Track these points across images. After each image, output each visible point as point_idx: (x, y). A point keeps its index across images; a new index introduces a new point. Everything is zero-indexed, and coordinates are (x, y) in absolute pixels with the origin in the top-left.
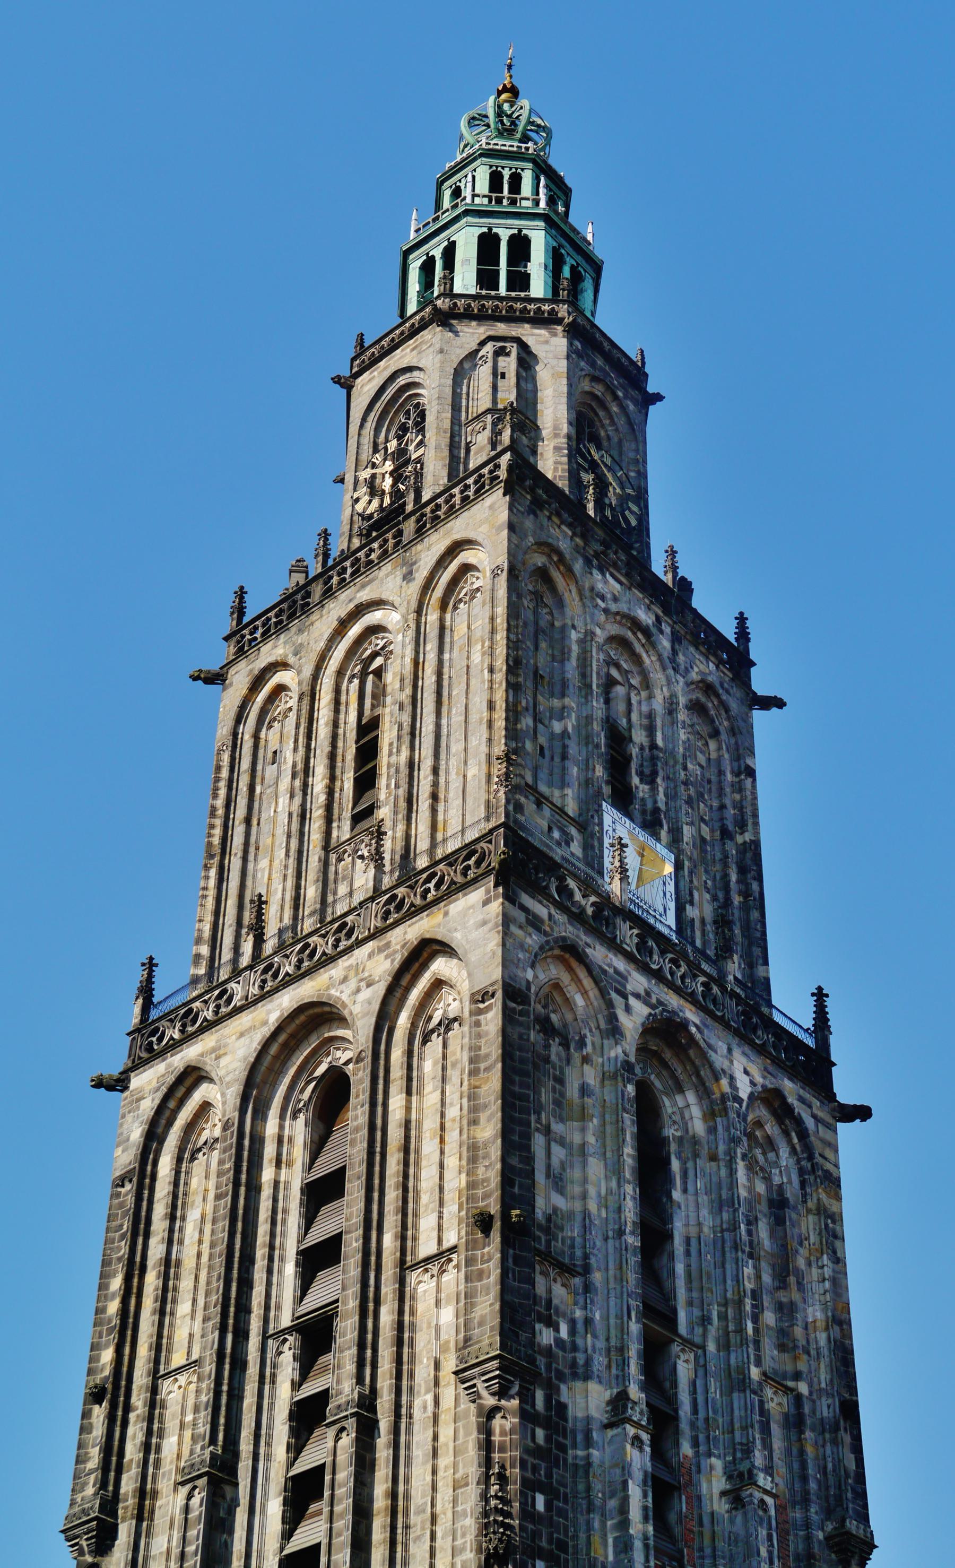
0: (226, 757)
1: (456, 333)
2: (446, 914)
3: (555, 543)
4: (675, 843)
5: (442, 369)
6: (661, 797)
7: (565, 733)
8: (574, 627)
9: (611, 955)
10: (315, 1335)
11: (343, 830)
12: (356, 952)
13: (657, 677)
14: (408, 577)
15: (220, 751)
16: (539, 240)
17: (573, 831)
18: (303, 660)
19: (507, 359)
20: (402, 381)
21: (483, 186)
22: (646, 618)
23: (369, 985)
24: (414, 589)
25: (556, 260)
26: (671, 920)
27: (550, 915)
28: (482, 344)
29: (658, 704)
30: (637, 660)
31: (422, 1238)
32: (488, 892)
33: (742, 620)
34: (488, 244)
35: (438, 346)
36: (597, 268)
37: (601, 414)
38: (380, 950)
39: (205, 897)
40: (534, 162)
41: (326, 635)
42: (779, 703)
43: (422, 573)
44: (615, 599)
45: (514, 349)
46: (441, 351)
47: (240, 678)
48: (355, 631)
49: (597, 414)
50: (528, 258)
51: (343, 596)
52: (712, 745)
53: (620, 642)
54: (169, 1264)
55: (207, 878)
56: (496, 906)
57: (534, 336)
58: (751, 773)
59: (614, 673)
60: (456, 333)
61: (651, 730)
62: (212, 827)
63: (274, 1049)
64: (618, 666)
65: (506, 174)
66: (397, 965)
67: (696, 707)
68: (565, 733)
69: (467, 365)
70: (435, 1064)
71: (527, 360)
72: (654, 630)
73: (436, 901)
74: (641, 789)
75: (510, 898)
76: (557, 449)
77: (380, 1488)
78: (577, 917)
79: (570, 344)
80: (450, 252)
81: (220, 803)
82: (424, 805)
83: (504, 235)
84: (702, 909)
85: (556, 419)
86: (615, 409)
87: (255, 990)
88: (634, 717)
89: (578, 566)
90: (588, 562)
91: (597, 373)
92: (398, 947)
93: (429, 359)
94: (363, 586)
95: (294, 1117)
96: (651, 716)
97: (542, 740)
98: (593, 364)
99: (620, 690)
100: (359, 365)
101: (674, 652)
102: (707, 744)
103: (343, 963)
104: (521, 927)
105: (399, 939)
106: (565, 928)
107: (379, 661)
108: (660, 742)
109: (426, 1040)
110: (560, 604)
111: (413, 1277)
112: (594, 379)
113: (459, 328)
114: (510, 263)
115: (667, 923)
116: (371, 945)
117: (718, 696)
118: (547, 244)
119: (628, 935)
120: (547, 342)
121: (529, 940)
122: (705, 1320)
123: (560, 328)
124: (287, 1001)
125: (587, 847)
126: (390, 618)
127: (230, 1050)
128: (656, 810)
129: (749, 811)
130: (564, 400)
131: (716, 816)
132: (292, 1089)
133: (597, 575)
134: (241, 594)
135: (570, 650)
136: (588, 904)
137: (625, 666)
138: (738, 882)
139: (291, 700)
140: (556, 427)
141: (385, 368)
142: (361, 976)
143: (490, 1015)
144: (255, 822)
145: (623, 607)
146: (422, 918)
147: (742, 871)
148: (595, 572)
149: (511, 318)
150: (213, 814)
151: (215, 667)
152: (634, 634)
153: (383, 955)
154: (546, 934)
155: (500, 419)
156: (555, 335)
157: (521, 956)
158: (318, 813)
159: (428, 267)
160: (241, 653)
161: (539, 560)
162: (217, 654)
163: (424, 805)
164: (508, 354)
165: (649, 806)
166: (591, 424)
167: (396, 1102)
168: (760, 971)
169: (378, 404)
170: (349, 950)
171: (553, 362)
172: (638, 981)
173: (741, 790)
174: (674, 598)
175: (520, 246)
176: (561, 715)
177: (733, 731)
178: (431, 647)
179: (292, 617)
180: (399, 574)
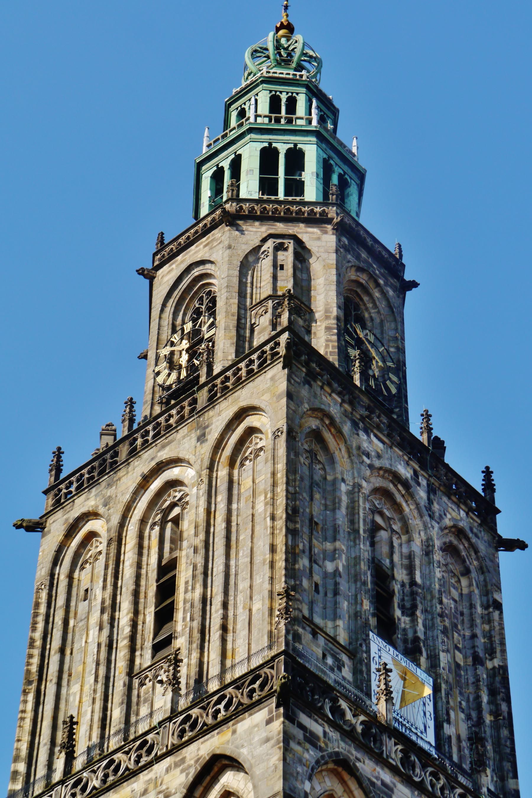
0: (44, 595)
1: (242, 232)
2: (234, 732)
3: (326, 409)
4: (433, 668)
5: (230, 263)
6: (420, 627)
7: (336, 572)
8: (343, 480)
9: (378, 769)
11: (144, 658)
12: (156, 767)
13: (415, 522)
14: (202, 438)
15: (39, 590)
17: (344, 658)
18: (111, 511)
19: (285, 253)
20: (196, 272)
21: (264, 108)
22: (405, 472)
25: (326, 169)
26: (431, 737)
27: (325, 733)
28: (264, 240)
29: (417, 547)
30: (398, 508)
32: (270, 712)
33: (488, 473)
34: (268, 157)
35: (226, 243)
36: (361, 176)
37: (366, 298)
38: (177, 765)
39: (22, 719)
40: (307, 87)
41: (132, 489)
42: (522, 545)
43: (213, 436)
44: (379, 456)
45: (291, 245)
46: (230, 247)
47: (57, 526)
49: (362, 299)
50: (302, 168)
51: (146, 455)
52: (464, 582)
53: (383, 493)
55: (25, 702)
56: (278, 725)
57: (308, 234)
58: (498, 606)
59: (379, 520)
60: (242, 232)
61: (410, 569)
62: (31, 656)
64: (381, 514)
65: (284, 97)
66: (191, 778)
67: (449, 549)
68: (337, 570)
69: (251, 259)
71: (302, 254)
72: (412, 483)
73: (226, 721)
74: (404, 621)
75: (290, 717)
78: (349, 734)
79: (339, 240)
81: (38, 635)
82: (215, 635)
83: (282, 149)
84: (458, 727)
85: (327, 304)
86: (377, 294)
88: (396, 558)
89: (347, 428)
90: (355, 425)
91: (362, 265)
92: (192, 762)
93: (220, 252)
94: (163, 447)
96: (410, 557)
97: (317, 578)
98: (358, 257)
99: (383, 535)
100: (160, 259)
101: (430, 502)
102: (459, 581)
103: (144, 777)
104: (299, 744)
105: (193, 755)
106: (338, 745)
107: (176, 511)
108: (418, 580)
110: (332, 460)
112: (359, 269)
113: (244, 227)
114: (286, 173)
115: (428, 740)
117: (468, 539)
118: (318, 156)
119: (393, 750)
120: (319, 239)
121: (306, 756)
123: (330, 227)
125: (356, 671)
126: (186, 474)
128: (416, 639)
129: (497, 639)
130: (334, 287)
131: (468, 644)
133: (363, 436)
134: (59, 454)
135: (340, 500)
136: (358, 722)
137: (387, 513)
138: (489, 703)
139: (100, 545)
140: (327, 311)
141: (182, 262)
142: (160, 789)
144: (68, 652)
145: (385, 463)
146: (213, 736)
147: (493, 693)
148: (361, 433)
149: (289, 218)
150: (32, 645)
151: (35, 517)
152: (395, 486)
153: (178, 770)
154: (321, 749)
155: (280, 304)
156: (326, 232)
157: (299, 769)
158: (123, 643)
160: (58, 504)
161: (313, 423)
162: (36, 506)
163: (215, 635)
164: (286, 249)
165: (410, 635)
166: (357, 307)
168: (511, 783)
169: (176, 292)
170: (149, 765)
171: (324, 256)
173: (489, 621)
174: (430, 455)
175: (296, 158)
176: (333, 556)
177: (482, 570)
178: (221, 499)
179: (102, 473)
180: (194, 436)
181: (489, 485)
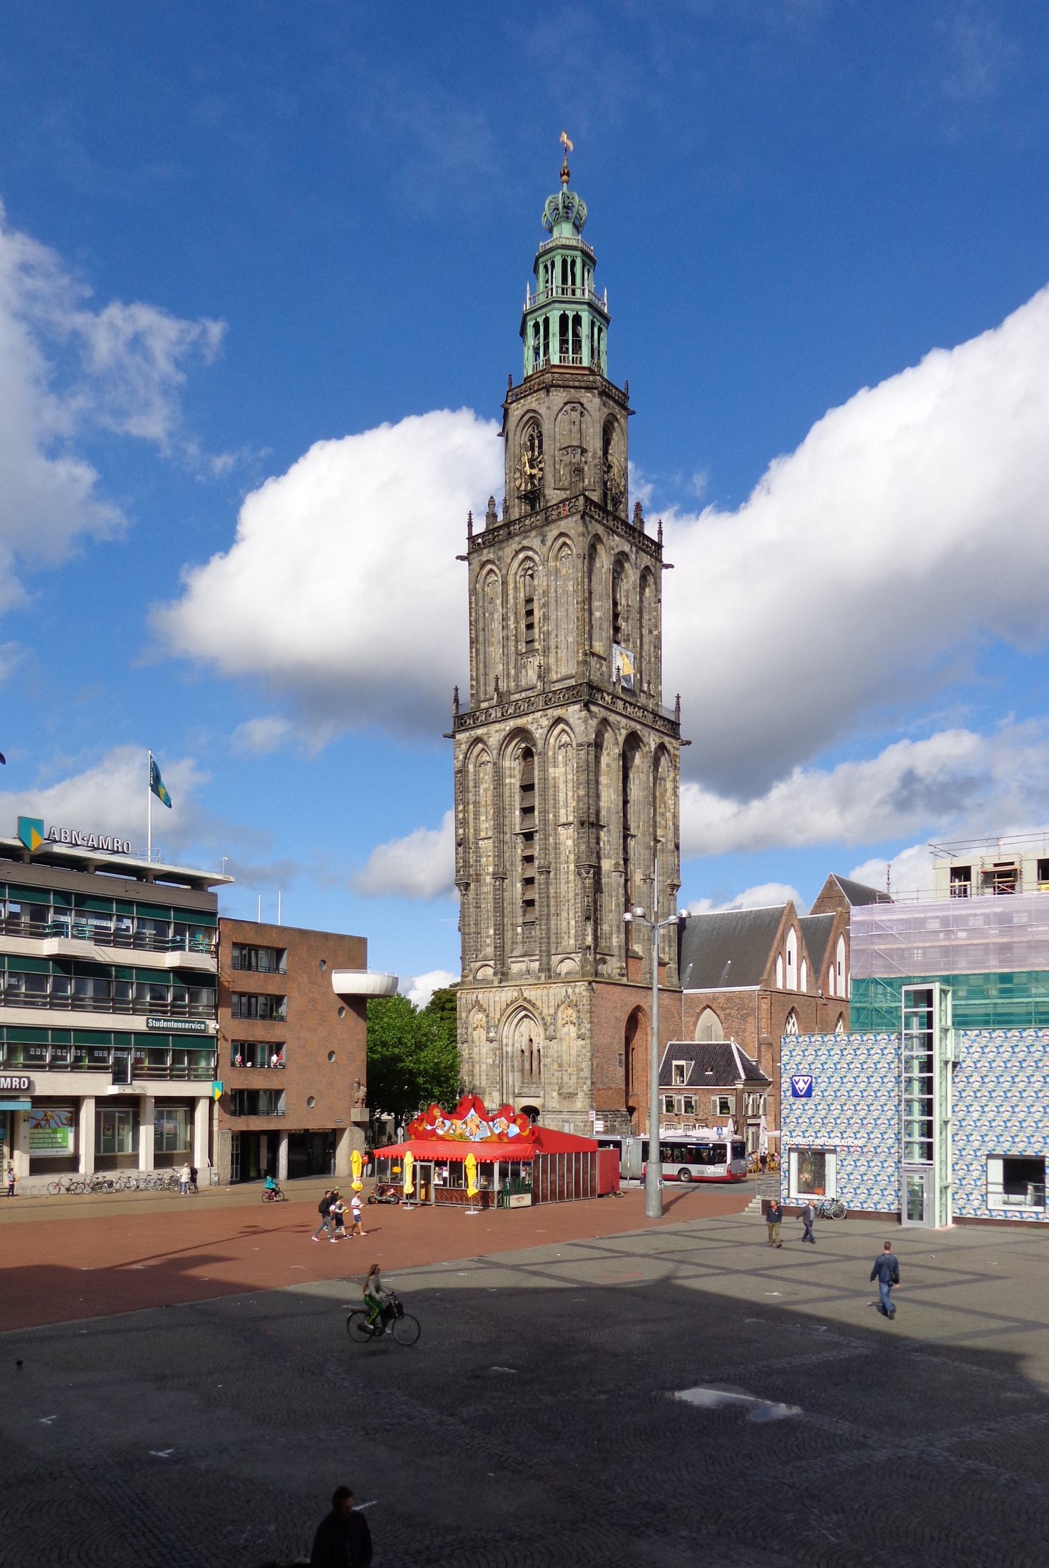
10: (529, 836)
14: (543, 542)
16: (586, 317)
24: (545, 549)
25: (593, 324)
34: (564, 318)
48: (521, 556)
65: (569, 260)
76: (595, 465)
77: (552, 891)
80: (546, 321)
83: (571, 314)
85: (594, 448)
94: (525, 538)
103: (531, 716)
124: (512, 724)
132: (515, 748)
140: (595, 453)
156: (594, 396)
159: (536, 326)
167: (551, 770)
172: (624, 721)
175: (577, 320)
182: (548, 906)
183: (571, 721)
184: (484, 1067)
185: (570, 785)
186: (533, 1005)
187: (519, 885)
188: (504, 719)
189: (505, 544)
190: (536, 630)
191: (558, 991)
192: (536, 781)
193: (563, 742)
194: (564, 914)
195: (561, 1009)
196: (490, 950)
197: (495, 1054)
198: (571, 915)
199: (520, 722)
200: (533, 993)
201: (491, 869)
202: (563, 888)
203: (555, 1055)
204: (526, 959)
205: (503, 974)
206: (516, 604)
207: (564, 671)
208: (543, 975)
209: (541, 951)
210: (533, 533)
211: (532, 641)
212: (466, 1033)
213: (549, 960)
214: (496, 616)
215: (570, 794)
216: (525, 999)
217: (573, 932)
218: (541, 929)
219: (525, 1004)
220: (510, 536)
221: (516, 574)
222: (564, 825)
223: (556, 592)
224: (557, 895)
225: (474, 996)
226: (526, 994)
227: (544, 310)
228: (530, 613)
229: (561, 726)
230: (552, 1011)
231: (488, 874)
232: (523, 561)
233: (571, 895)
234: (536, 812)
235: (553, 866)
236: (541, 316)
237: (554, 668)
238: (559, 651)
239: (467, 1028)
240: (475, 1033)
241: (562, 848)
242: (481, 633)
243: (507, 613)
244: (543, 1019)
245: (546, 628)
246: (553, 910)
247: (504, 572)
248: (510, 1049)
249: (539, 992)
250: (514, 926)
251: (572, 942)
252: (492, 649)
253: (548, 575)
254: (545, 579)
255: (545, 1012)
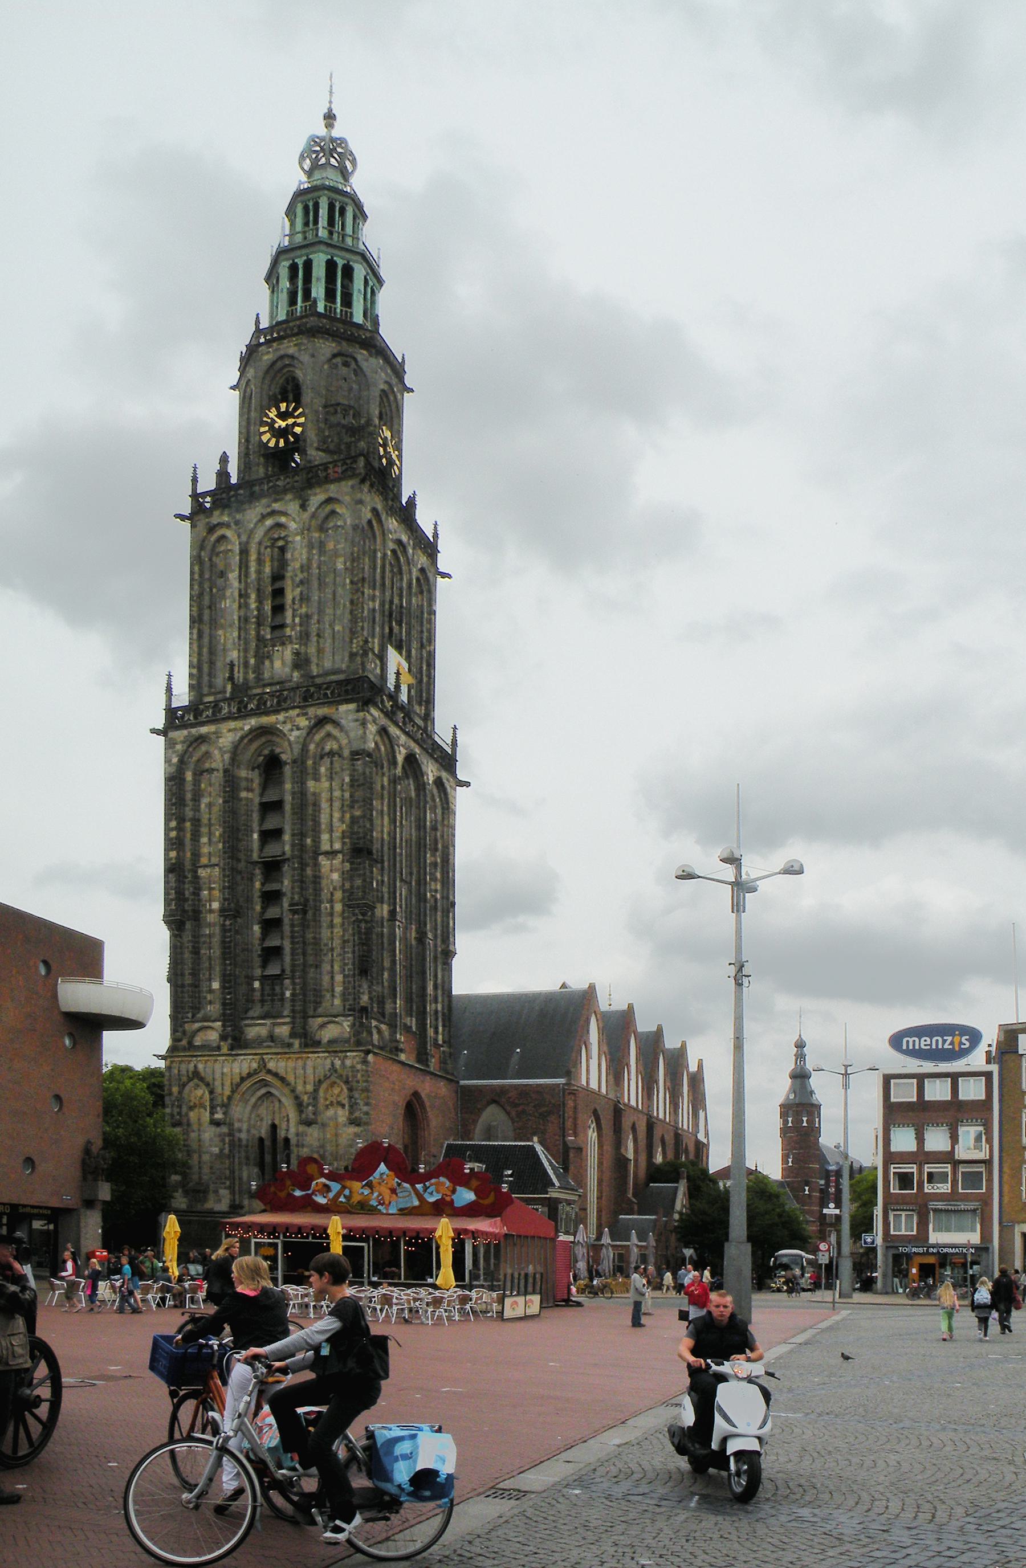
10: (272, 868)
14: (303, 507)
23: (298, 729)
24: (306, 516)
28: (334, 356)
31: (323, 842)
43: (312, 509)
48: (269, 522)
54: (196, 822)
63: (246, 741)
70: (327, 770)
80: (308, 265)
87: (235, 710)
94: (276, 501)
95: (253, 769)
96: (401, 589)
109: (322, 757)
111: (321, 858)
116: (297, 711)
122: (411, 874)
127: (228, 735)
141: (277, 350)
143: (359, 762)
153: (304, 718)
167: (311, 784)
181: (436, 535)
182: (304, 954)
183: (343, 722)
184: (206, 1158)
185: (337, 804)
186: (283, 1079)
187: (256, 928)
188: (242, 714)
189: (246, 506)
190: (289, 613)
191: (317, 1063)
192: (288, 798)
193: (328, 748)
194: (326, 967)
195: (324, 1086)
196: (213, 1009)
197: (223, 1141)
198: (336, 968)
199: (265, 720)
200: (282, 1064)
201: (216, 905)
202: (325, 933)
203: (316, 1144)
204: (268, 1022)
205: (235, 1039)
206: (259, 580)
207: (328, 664)
208: (297, 1043)
209: (293, 1011)
210: (289, 496)
211: (282, 626)
212: (179, 1114)
213: (305, 1024)
214: (228, 593)
215: (337, 815)
216: (269, 1072)
217: (338, 989)
218: (294, 983)
219: (269, 1078)
220: (253, 497)
221: (260, 543)
222: (326, 853)
223: (319, 568)
224: (317, 941)
225: (192, 1065)
226: (271, 1065)
227: (304, 251)
228: (279, 593)
229: (329, 728)
230: (310, 1088)
231: (211, 911)
232: (272, 528)
233: (337, 943)
234: (287, 837)
235: (311, 902)
236: (300, 257)
237: (314, 660)
238: (321, 641)
239: (180, 1107)
240: (191, 1114)
241: (324, 882)
242: (207, 612)
243: (246, 589)
244: (297, 1098)
245: (304, 610)
246: (311, 960)
247: (244, 538)
248: (243, 1136)
249: (291, 1064)
250: (250, 979)
251: (337, 1002)
252: (220, 632)
253: (310, 546)
254: (304, 551)
255: (300, 1088)
